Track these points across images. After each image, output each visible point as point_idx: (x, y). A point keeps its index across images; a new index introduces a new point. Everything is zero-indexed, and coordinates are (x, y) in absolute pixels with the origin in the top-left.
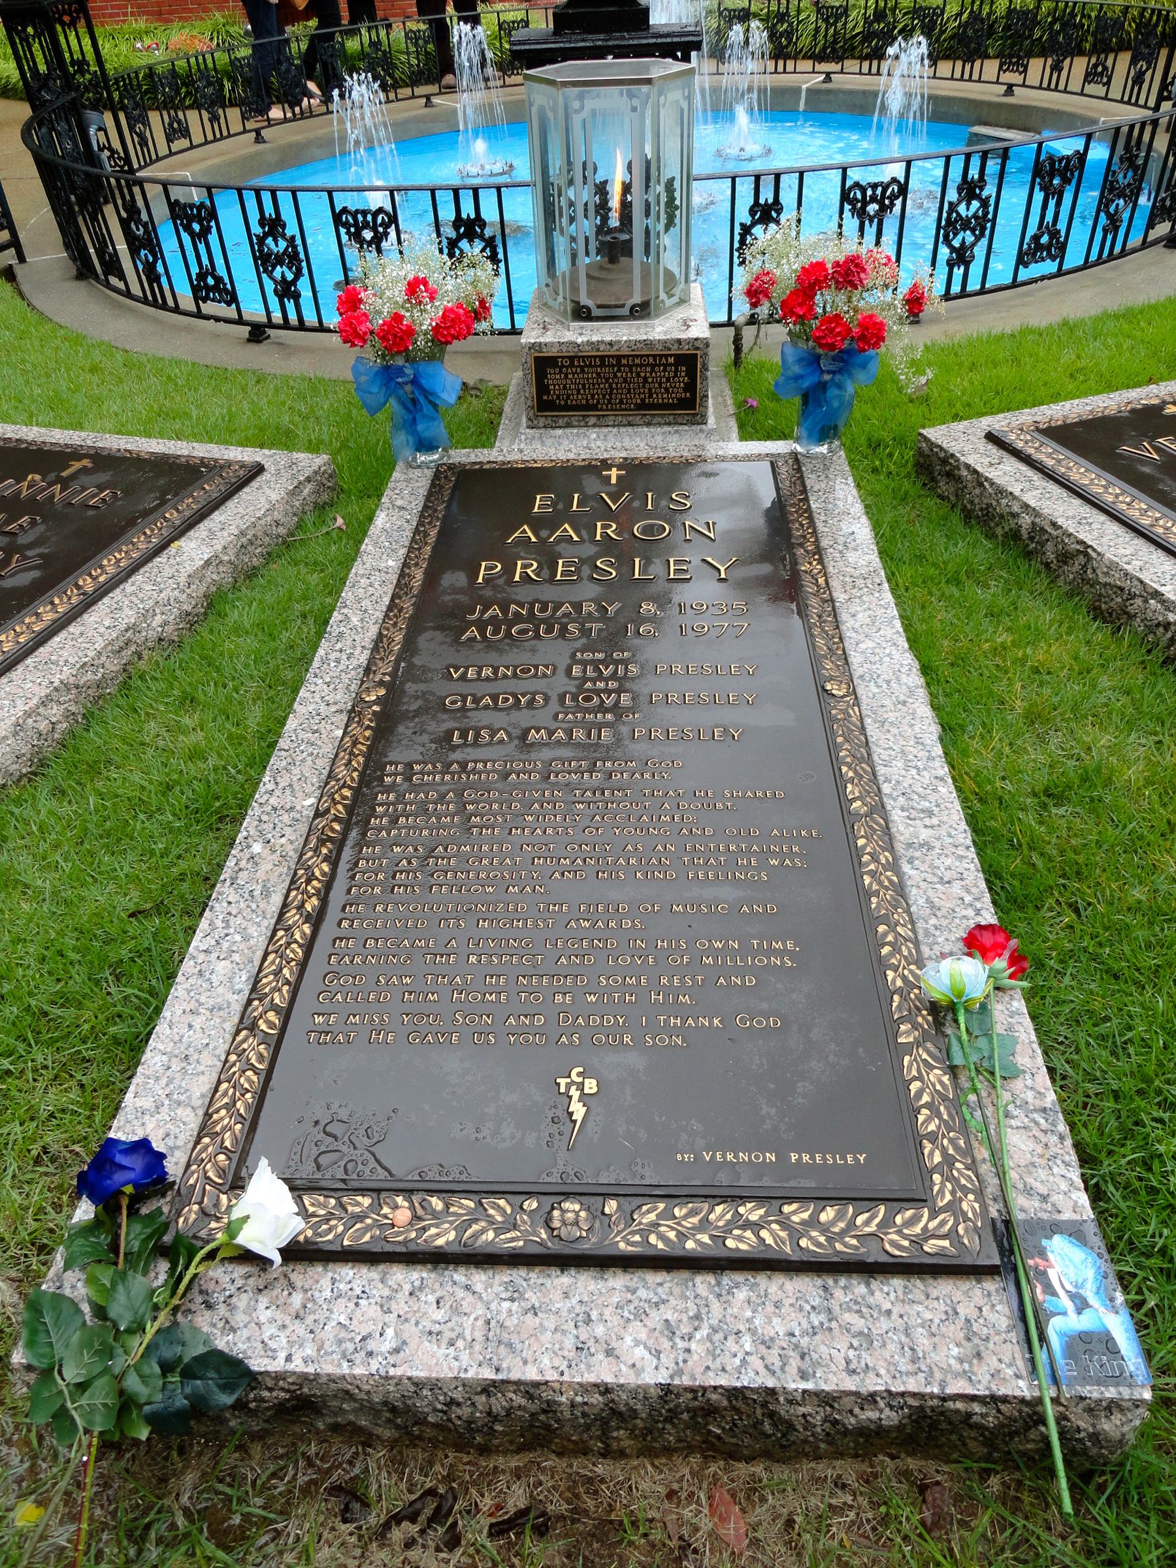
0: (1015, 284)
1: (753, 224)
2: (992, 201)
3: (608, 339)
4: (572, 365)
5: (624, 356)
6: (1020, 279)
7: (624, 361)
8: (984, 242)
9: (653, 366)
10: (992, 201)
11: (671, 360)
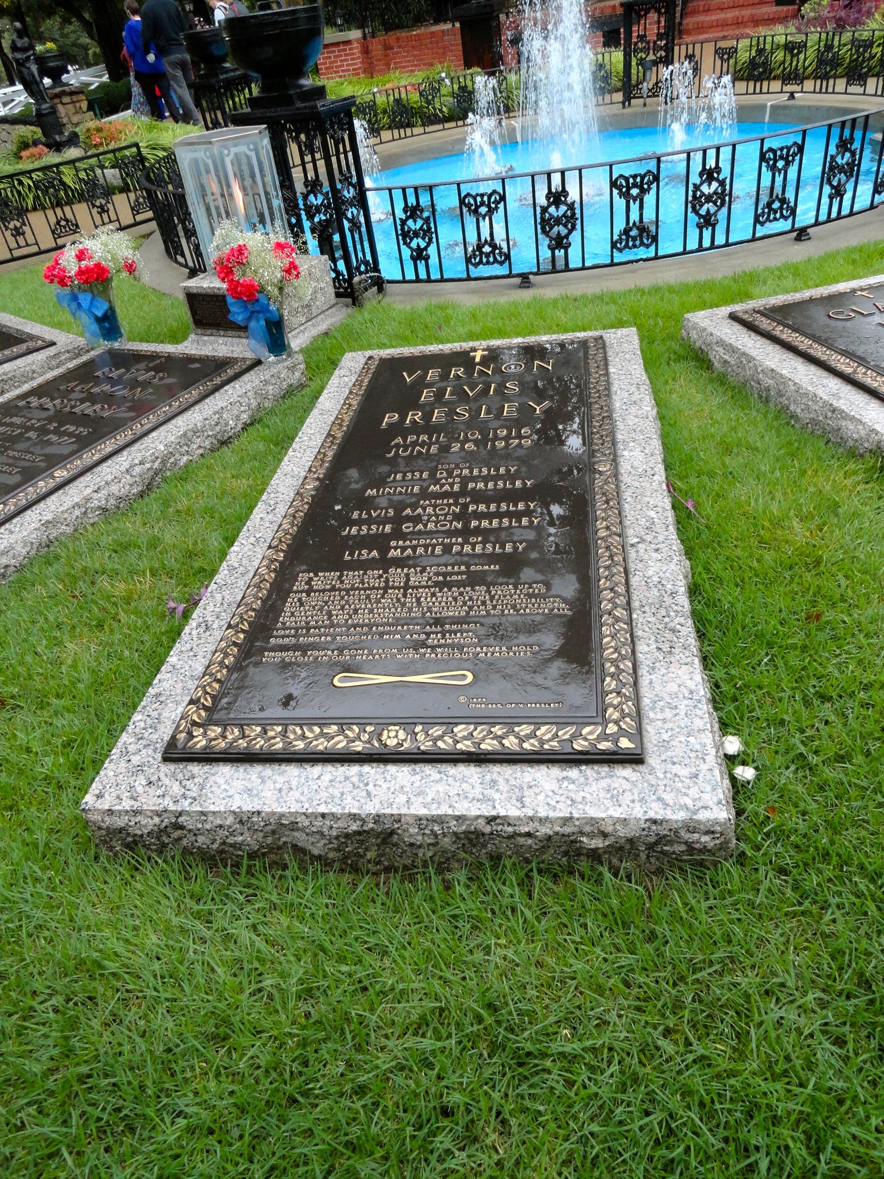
0: (754, 239)
1: (549, 206)
2: (728, 181)
6: (758, 235)
8: (725, 210)
10: (728, 181)
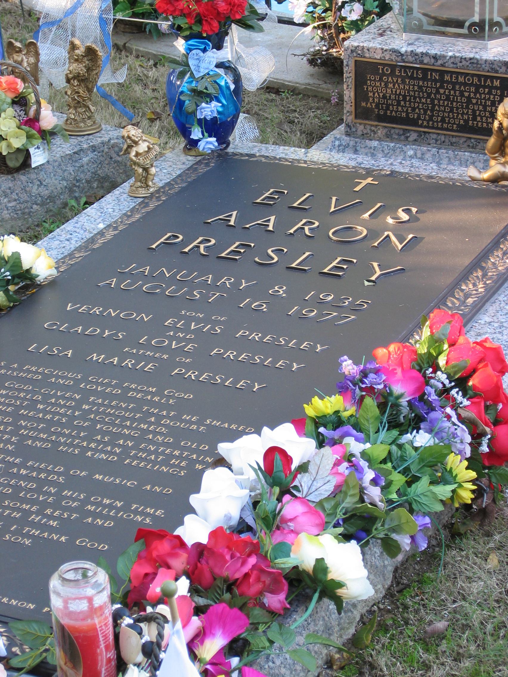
3: (433, 52)
4: (392, 74)
5: (447, 72)
7: (447, 78)
9: (477, 87)
11: (497, 83)
